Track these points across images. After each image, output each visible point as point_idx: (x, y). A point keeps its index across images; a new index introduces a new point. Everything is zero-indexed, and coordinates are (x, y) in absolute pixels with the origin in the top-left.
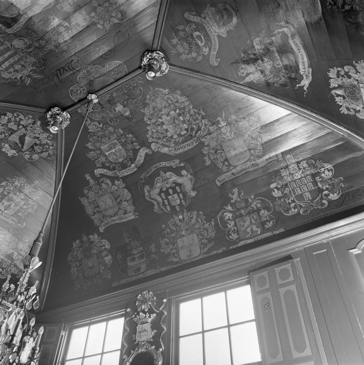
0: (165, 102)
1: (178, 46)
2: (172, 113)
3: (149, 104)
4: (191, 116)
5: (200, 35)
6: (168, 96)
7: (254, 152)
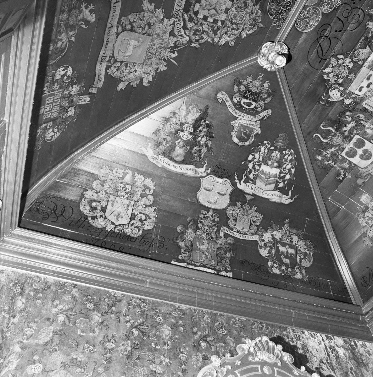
0: (239, 22)
1: (260, 84)
2: (223, 17)
3: (254, 5)
4: (204, 31)
5: (250, 107)
6: (240, 30)
7: (116, 66)
